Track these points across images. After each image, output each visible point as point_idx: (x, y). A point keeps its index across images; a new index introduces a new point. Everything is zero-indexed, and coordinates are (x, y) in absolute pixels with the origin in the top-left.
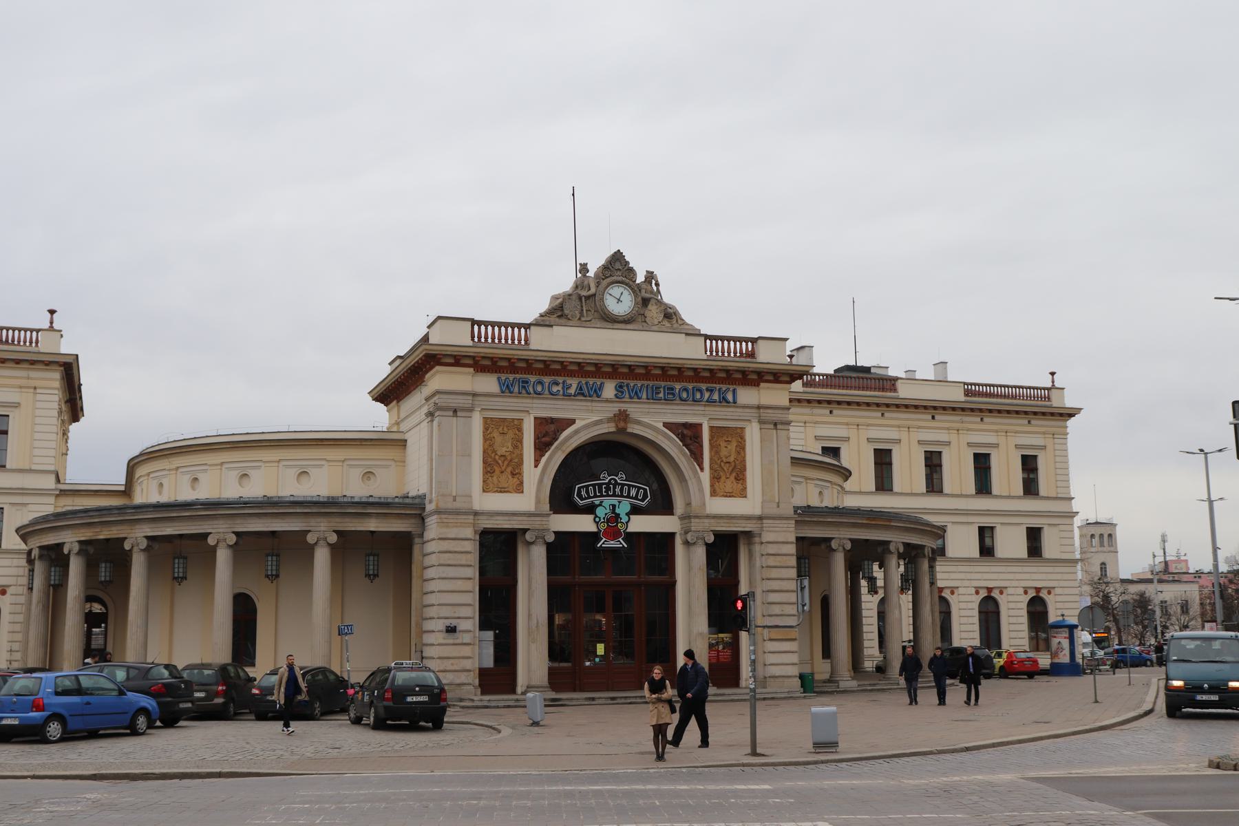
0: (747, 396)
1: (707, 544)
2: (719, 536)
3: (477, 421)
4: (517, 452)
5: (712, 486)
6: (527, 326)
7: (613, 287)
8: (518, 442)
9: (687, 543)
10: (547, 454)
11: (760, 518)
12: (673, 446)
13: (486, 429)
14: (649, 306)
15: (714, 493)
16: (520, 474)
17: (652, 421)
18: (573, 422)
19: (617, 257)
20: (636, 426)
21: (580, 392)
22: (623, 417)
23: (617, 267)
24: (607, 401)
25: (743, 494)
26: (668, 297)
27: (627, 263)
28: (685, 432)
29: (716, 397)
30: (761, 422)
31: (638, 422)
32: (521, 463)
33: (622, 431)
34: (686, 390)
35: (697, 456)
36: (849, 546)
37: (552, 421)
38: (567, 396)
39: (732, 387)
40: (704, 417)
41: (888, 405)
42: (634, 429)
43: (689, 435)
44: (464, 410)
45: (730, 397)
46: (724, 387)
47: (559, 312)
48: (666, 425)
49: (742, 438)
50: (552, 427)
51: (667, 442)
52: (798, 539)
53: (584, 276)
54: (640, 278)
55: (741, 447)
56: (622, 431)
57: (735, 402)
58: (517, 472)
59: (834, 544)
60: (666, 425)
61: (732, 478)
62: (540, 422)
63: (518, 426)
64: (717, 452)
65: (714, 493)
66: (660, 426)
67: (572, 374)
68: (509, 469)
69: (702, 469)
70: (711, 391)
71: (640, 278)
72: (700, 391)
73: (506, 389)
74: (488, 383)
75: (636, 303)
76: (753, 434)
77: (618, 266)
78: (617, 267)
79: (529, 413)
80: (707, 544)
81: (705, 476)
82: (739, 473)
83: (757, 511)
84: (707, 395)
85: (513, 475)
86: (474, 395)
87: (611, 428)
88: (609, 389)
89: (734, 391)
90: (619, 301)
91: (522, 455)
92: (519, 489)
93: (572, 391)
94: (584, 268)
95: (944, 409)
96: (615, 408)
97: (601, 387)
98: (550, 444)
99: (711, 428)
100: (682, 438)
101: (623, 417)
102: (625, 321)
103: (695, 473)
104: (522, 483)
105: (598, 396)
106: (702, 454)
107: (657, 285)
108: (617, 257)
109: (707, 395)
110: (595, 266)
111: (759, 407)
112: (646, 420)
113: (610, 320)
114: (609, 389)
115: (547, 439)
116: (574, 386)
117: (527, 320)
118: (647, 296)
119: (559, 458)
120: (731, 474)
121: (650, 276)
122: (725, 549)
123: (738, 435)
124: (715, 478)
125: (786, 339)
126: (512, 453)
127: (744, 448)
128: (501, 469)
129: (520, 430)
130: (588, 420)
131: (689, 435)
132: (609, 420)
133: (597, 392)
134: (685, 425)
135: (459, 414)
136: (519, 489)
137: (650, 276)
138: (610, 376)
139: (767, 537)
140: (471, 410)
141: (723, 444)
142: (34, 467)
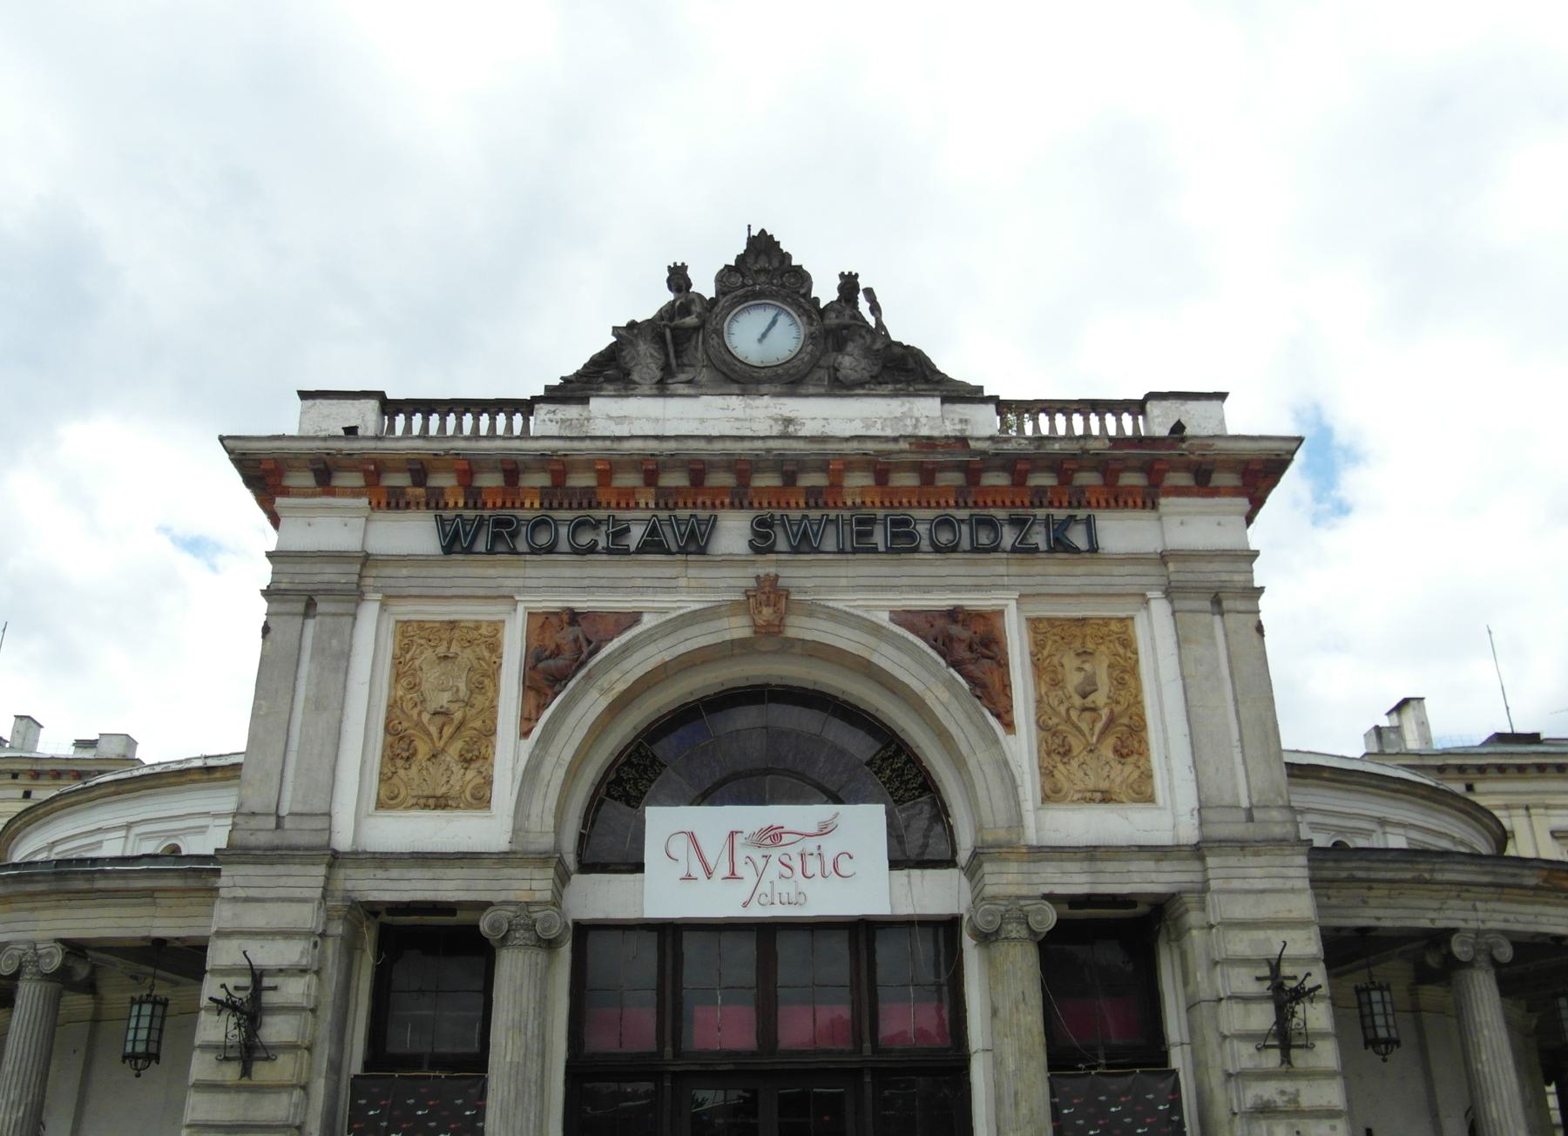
0: (1122, 532)
3: (370, 636)
4: (479, 701)
5: (1047, 773)
6: (526, 407)
7: (757, 310)
9: (986, 939)
11: (1198, 851)
14: (851, 344)
15: (1051, 795)
17: (860, 609)
18: (635, 618)
19: (762, 247)
21: (653, 544)
22: (770, 593)
24: (730, 561)
25: (1143, 794)
26: (900, 331)
28: (955, 630)
29: (1039, 538)
30: (1170, 592)
31: (811, 610)
33: (770, 637)
34: (946, 522)
35: (991, 694)
36: (1506, 953)
37: (574, 617)
38: (617, 549)
39: (1082, 514)
42: (801, 628)
43: (968, 645)
45: (1078, 537)
46: (1060, 514)
49: (1128, 643)
50: (570, 632)
55: (1126, 672)
56: (770, 637)
57: (1094, 549)
59: (1458, 948)
60: (905, 618)
61: (1107, 751)
62: (541, 622)
64: (1056, 683)
65: (1051, 795)
66: (883, 618)
67: (627, 499)
69: (1009, 726)
70: (1019, 522)
72: (991, 524)
73: (454, 542)
74: (414, 534)
75: (811, 337)
76: (1155, 631)
77: (763, 263)
79: (513, 603)
81: (1022, 746)
82: (1128, 736)
83: (1189, 833)
84: (1008, 537)
87: (737, 628)
88: (733, 531)
89: (1089, 523)
91: (493, 708)
92: (481, 799)
94: (678, 277)
96: (743, 578)
97: (712, 523)
98: (558, 680)
99: (1034, 623)
100: (944, 646)
101: (770, 593)
102: (789, 379)
105: (702, 551)
106: (1006, 686)
108: (762, 247)
109: (1008, 537)
111: (1164, 558)
112: (841, 602)
114: (733, 531)
119: (593, 704)
121: (849, 284)
122: (1107, 954)
125: (1222, 396)
126: (468, 704)
127: (1133, 669)
128: (429, 749)
129: (494, 647)
130: (673, 612)
131: (968, 645)
132: (734, 608)
133: (696, 542)
134: (954, 614)
135: (322, 607)
138: (739, 498)
139: (1225, 908)
140: (356, 595)
141: (1070, 662)
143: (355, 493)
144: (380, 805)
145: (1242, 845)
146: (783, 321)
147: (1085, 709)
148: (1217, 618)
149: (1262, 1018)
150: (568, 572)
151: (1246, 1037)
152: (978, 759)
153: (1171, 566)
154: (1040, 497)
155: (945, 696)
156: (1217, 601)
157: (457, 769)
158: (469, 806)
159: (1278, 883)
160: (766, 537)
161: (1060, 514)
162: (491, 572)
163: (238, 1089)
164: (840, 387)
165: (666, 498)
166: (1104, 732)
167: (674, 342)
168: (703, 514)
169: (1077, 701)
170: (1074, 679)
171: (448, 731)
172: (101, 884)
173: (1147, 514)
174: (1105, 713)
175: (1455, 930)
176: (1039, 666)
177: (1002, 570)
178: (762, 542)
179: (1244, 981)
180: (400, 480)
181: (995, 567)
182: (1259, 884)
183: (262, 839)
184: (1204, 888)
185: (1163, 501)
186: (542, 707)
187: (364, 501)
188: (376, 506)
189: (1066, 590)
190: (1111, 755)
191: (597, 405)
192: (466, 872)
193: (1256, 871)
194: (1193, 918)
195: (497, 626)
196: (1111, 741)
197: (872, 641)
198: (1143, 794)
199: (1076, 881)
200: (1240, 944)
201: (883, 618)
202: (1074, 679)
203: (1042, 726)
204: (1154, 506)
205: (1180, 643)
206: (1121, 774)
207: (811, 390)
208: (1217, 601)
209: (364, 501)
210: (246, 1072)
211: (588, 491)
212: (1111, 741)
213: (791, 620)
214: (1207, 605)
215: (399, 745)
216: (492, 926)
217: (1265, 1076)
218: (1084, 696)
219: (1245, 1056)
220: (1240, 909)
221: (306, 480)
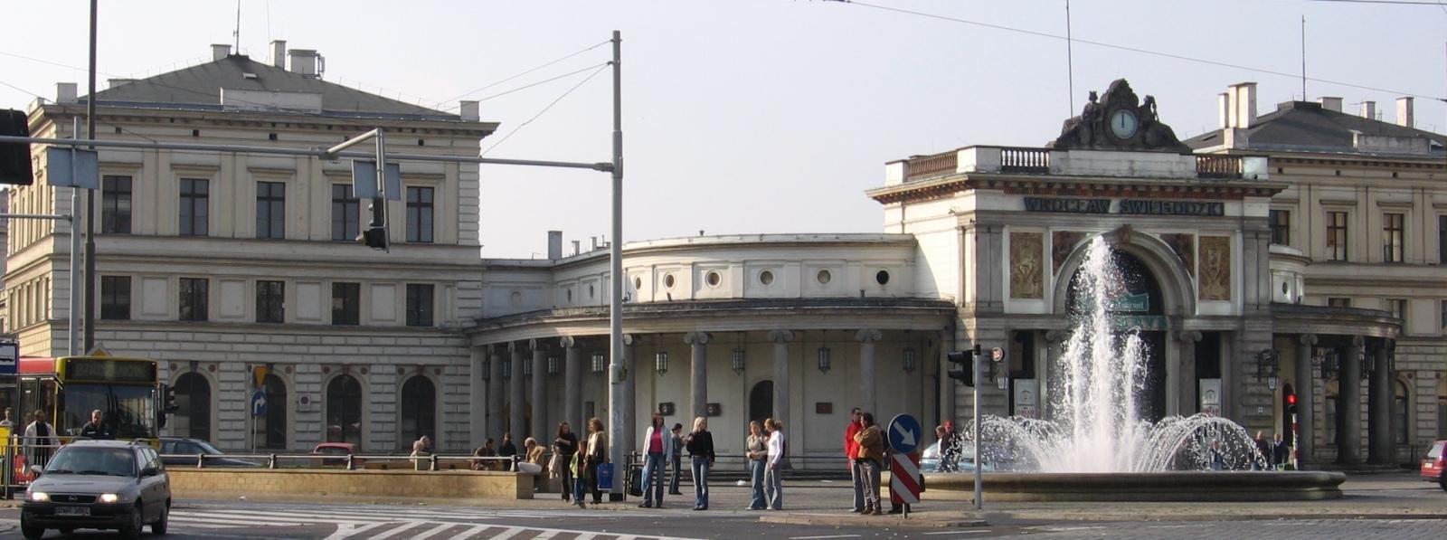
0: (1231, 209)
1: (1196, 342)
2: (1205, 334)
8: (1039, 253)
10: (1063, 265)
11: (1242, 318)
12: (1167, 255)
13: (1012, 242)
16: (1041, 281)
20: (1137, 238)
23: (1121, 92)
26: (1164, 117)
27: (1131, 90)
29: (1205, 211)
30: (1244, 231)
32: (1040, 271)
35: (1187, 264)
38: (1077, 211)
39: (1219, 201)
40: (1196, 232)
41: (1344, 163)
42: (1135, 240)
43: (1181, 245)
44: (995, 226)
45: (1218, 210)
46: (1214, 201)
47: (1073, 137)
48: (1163, 236)
51: (1161, 250)
52: (1275, 335)
53: (1094, 102)
54: (1141, 103)
55: (1226, 255)
57: (1222, 214)
58: (1038, 276)
59: (1302, 340)
60: (1163, 236)
63: (1038, 240)
65: (1202, 297)
67: (1084, 192)
68: (1031, 278)
69: (1193, 275)
71: (1141, 103)
73: (1031, 206)
74: (1014, 203)
75: (1139, 127)
76: (1237, 243)
78: (1121, 92)
80: (1196, 342)
81: (1195, 282)
82: (1225, 278)
83: (1239, 313)
85: (1034, 282)
86: (1003, 213)
88: (1114, 206)
90: (1123, 125)
93: (1083, 208)
95: (1408, 165)
97: (1109, 202)
98: (1064, 257)
99: (1200, 237)
100: (1175, 246)
103: (1188, 280)
104: (1042, 289)
105: (1107, 213)
106: (1193, 265)
107: (1155, 107)
110: (1102, 90)
111: (1242, 218)
113: (1116, 144)
114: (1114, 206)
115: (1064, 252)
116: (1087, 203)
117: (1042, 145)
118: (1146, 115)
120: (1218, 278)
121: (1150, 100)
123: (1225, 243)
124: (1203, 282)
127: (1228, 256)
134: (1178, 236)
136: (1040, 295)
137: (1150, 100)
140: (1002, 226)
141: (1210, 252)
142: (461, 243)
143: (1000, 189)
144: (1011, 297)
145: (1256, 317)
146: (1125, 115)
147: (1213, 268)
148: (1255, 241)
149: (1255, 369)
150: (1064, 218)
151: (1250, 374)
152: (1183, 286)
153: (1245, 222)
154: (1208, 196)
155: (1175, 265)
156: (1257, 235)
157: (1033, 285)
158: (1036, 298)
159: (1264, 329)
160: (1126, 209)
161: (1214, 201)
162: (1041, 217)
163: (990, 385)
164: (1148, 147)
165: (1096, 192)
166: (1218, 276)
167: (1090, 128)
168: (1105, 198)
169: (1211, 265)
170: (1211, 258)
171: (1028, 272)
172: (898, 312)
173: (1239, 202)
174: (1218, 270)
175: (1302, 334)
176: (1203, 256)
177: (1194, 221)
178: (1125, 209)
179: (1251, 358)
180: (1014, 185)
181: (1192, 220)
182: (1259, 329)
183: (984, 310)
184: (1242, 330)
185: (1245, 198)
186: (1060, 265)
187: (1002, 191)
188: (1006, 192)
189: (1214, 229)
190: (1218, 284)
191: (1073, 154)
192: (1042, 320)
193: (1257, 326)
194: (1239, 337)
195: (1040, 236)
196: (1219, 279)
197: (1156, 246)
198: (1227, 297)
199: (1208, 326)
200: (1251, 348)
201: (1157, 237)
202: (1211, 258)
203: (1200, 274)
204: (1242, 199)
205: (1245, 249)
206: (1221, 290)
207: (1140, 149)
208: (1257, 235)
209: (1002, 191)
210: (991, 380)
211: (1072, 190)
212: (1219, 279)
213: (1132, 237)
214: (1253, 236)
215: (1014, 280)
216: (1050, 337)
217: (1254, 385)
218: (1213, 264)
219: (1250, 380)
220: (1252, 337)
221: (986, 184)
